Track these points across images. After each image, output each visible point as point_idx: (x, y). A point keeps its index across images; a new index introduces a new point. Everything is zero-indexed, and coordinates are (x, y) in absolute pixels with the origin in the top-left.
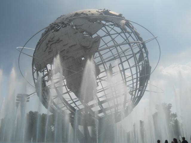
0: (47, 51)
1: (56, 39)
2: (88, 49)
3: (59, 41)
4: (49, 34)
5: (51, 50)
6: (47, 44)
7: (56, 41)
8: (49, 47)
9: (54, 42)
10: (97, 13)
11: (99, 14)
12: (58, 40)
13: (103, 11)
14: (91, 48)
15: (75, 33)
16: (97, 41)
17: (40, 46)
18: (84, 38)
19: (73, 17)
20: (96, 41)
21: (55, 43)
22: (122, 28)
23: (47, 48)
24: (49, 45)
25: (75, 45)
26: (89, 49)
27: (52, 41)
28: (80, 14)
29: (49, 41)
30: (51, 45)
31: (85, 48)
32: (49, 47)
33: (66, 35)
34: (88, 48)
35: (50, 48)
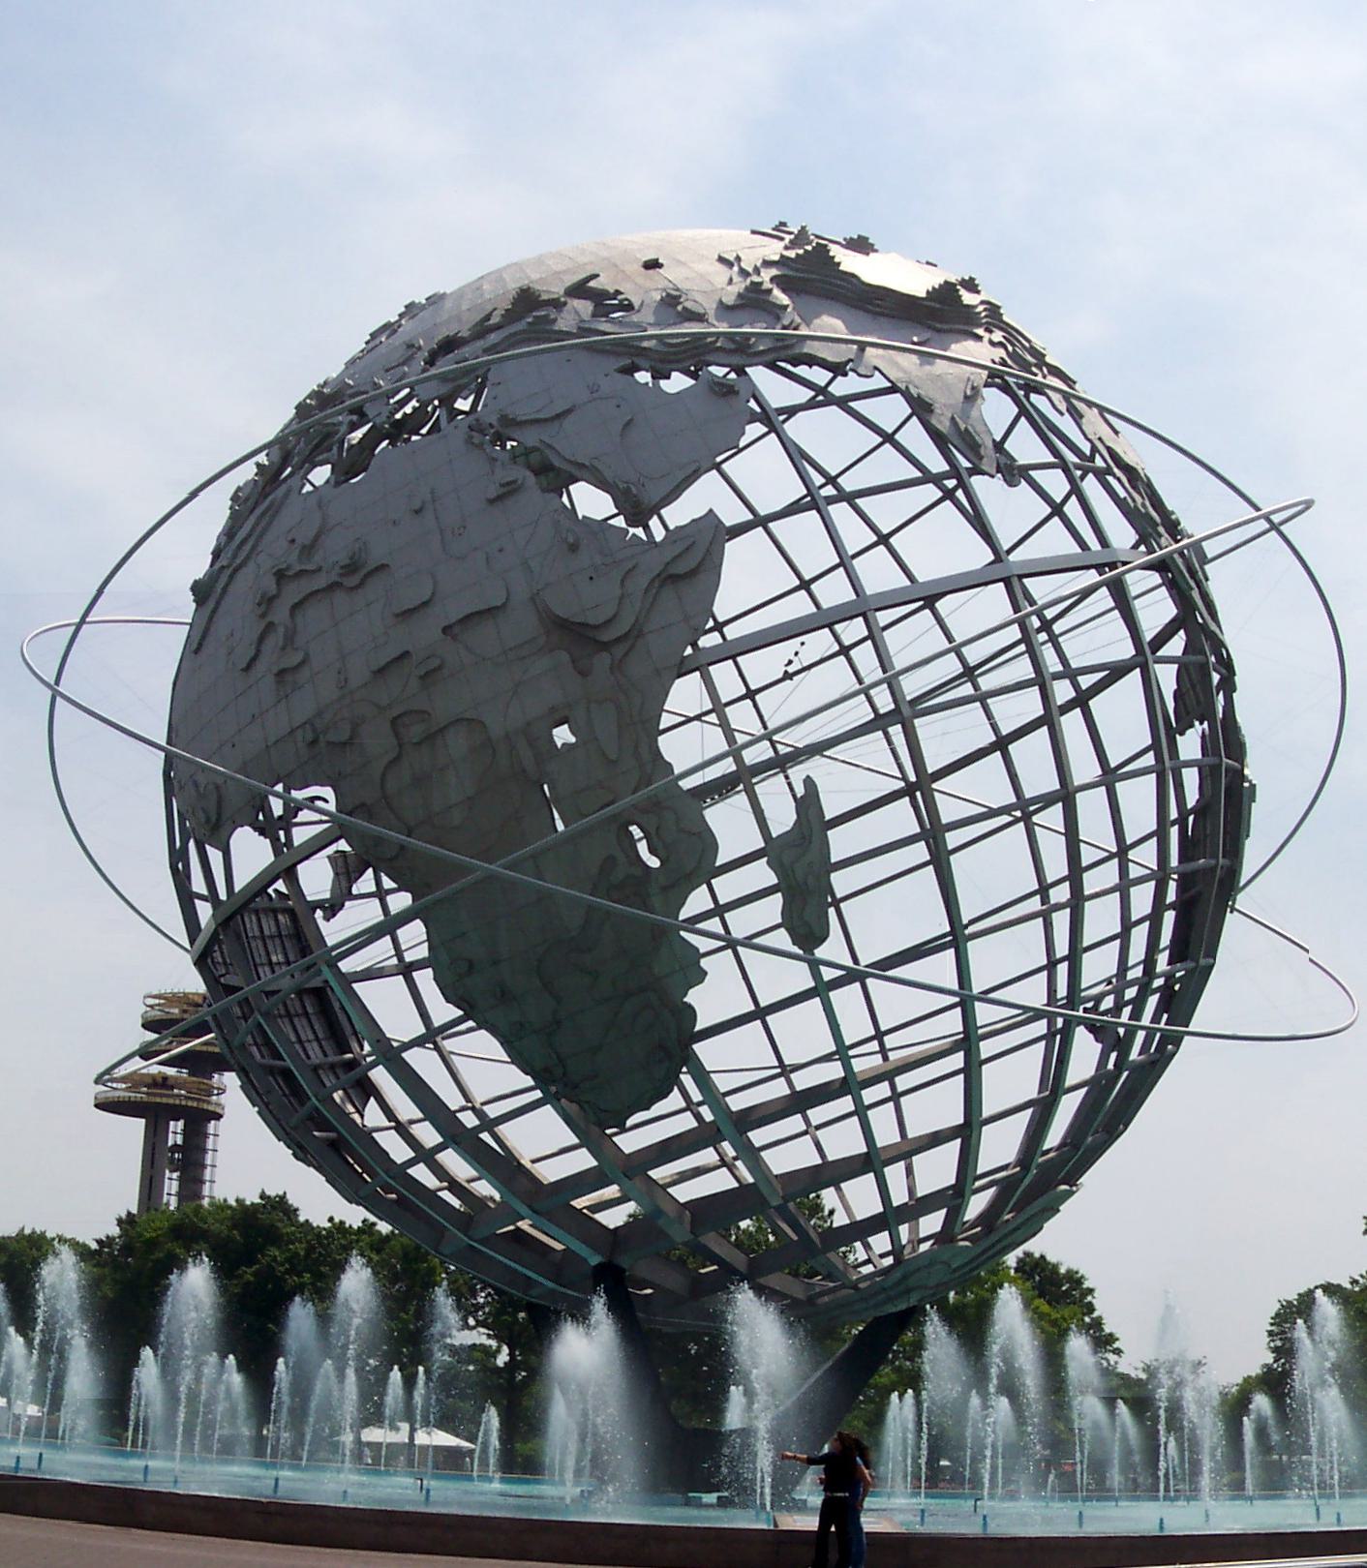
0: (261, 667)
1: (335, 551)
2: (605, 646)
3: (357, 572)
4: (282, 503)
5: (295, 659)
6: (268, 601)
7: (334, 578)
8: (281, 630)
9: (321, 582)
10: (721, 274)
11: (740, 285)
12: (351, 568)
13: (783, 261)
14: (635, 633)
15: (500, 498)
16: (693, 573)
17: (214, 611)
18: (574, 548)
19: (498, 327)
20: (681, 568)
21: (333, 587)
22: (943, 425)
23: (261, 639)
24: (280, 614)
25: (490, 612)
26: (619, 651)
27: (302, 573)
28: (557, 304)
29: (281, 576)
30: (299, 619)
31: (577, 637)
32: (281, 630)
33: (417, 512)
34: (606, 636)
35: (290, 639)
